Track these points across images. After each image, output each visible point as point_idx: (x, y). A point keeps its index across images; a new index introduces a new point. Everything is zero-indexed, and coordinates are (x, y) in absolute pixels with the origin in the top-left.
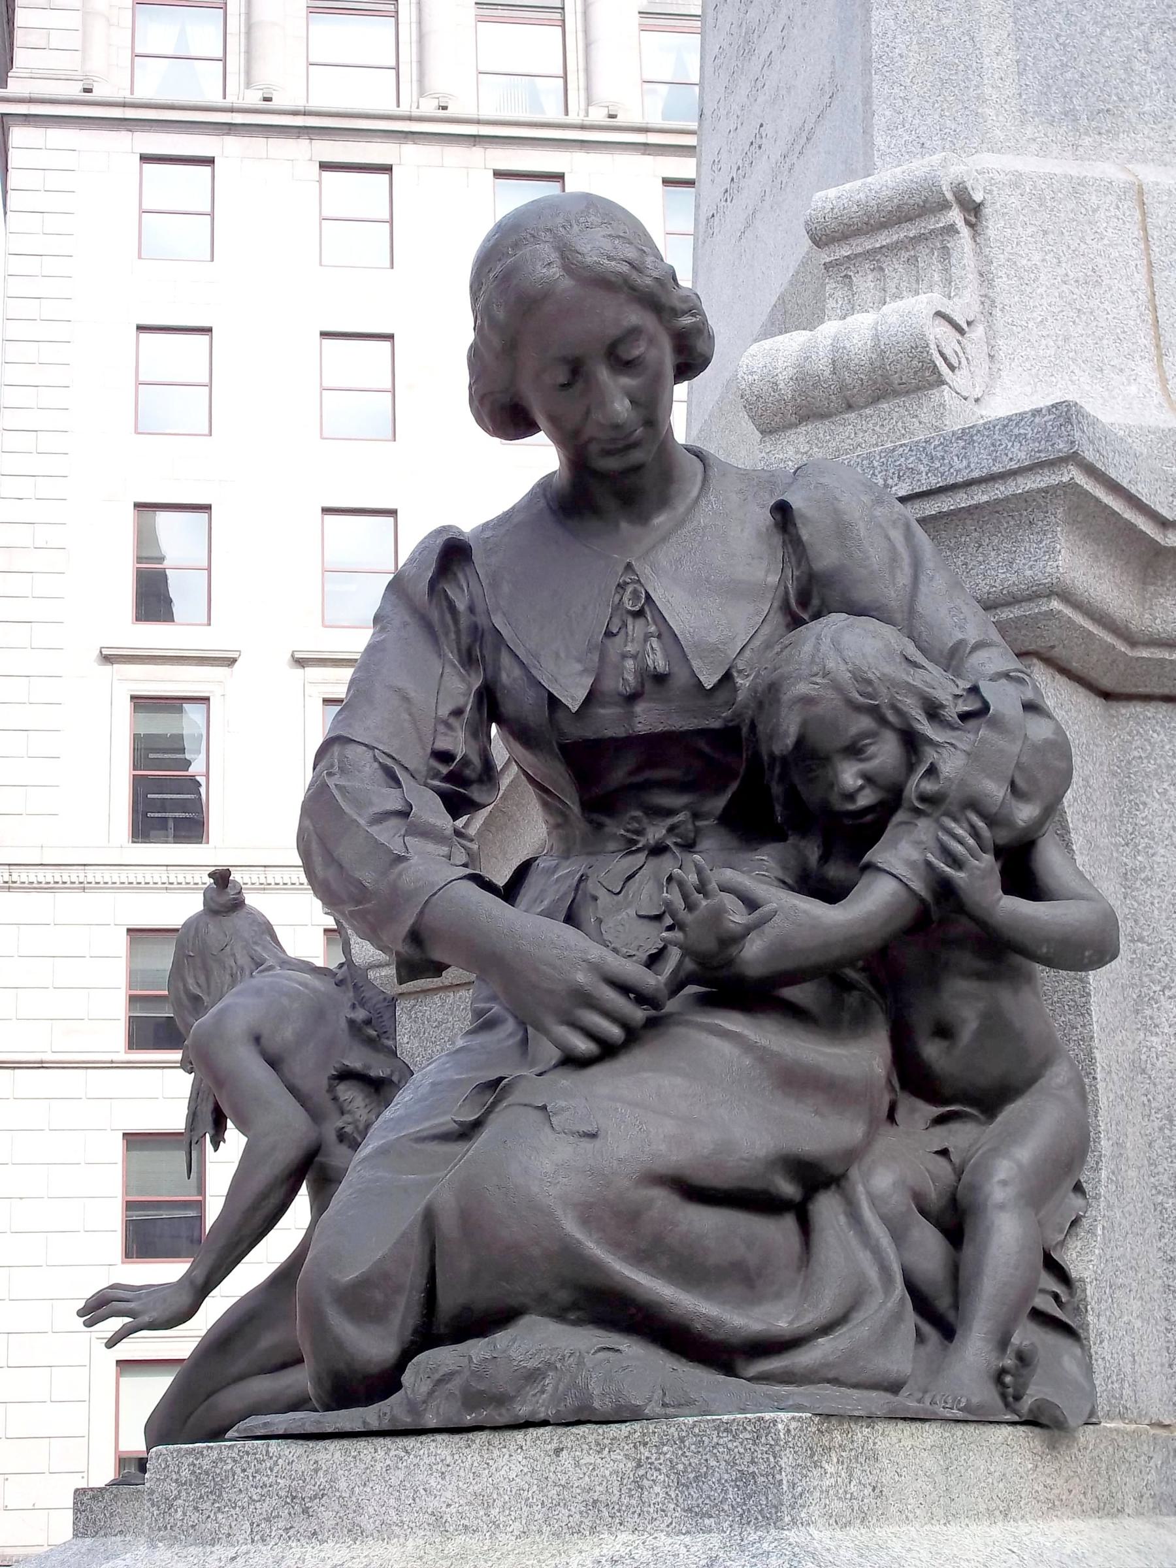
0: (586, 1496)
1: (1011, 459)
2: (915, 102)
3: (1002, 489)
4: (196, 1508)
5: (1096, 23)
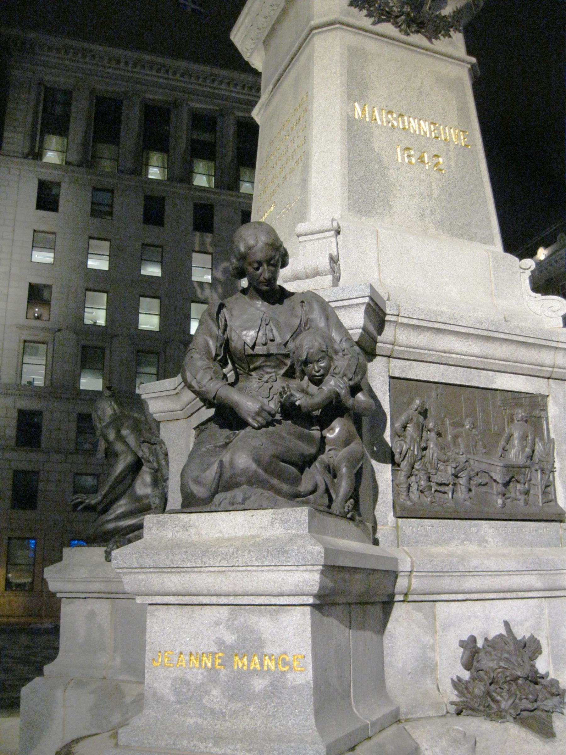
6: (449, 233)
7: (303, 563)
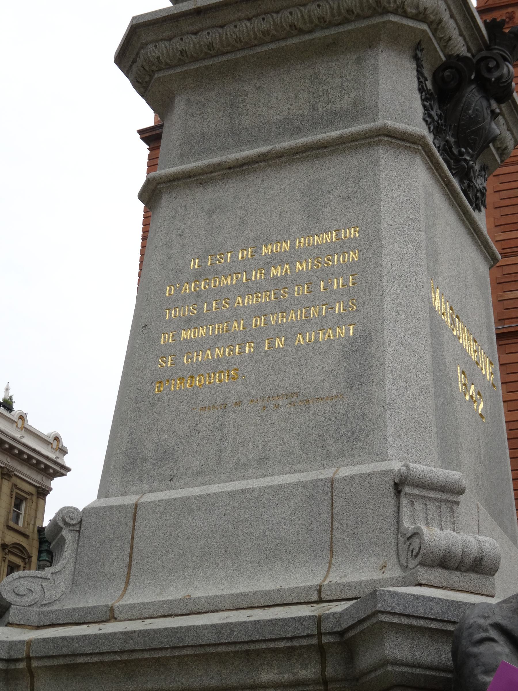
2: (405, 430)
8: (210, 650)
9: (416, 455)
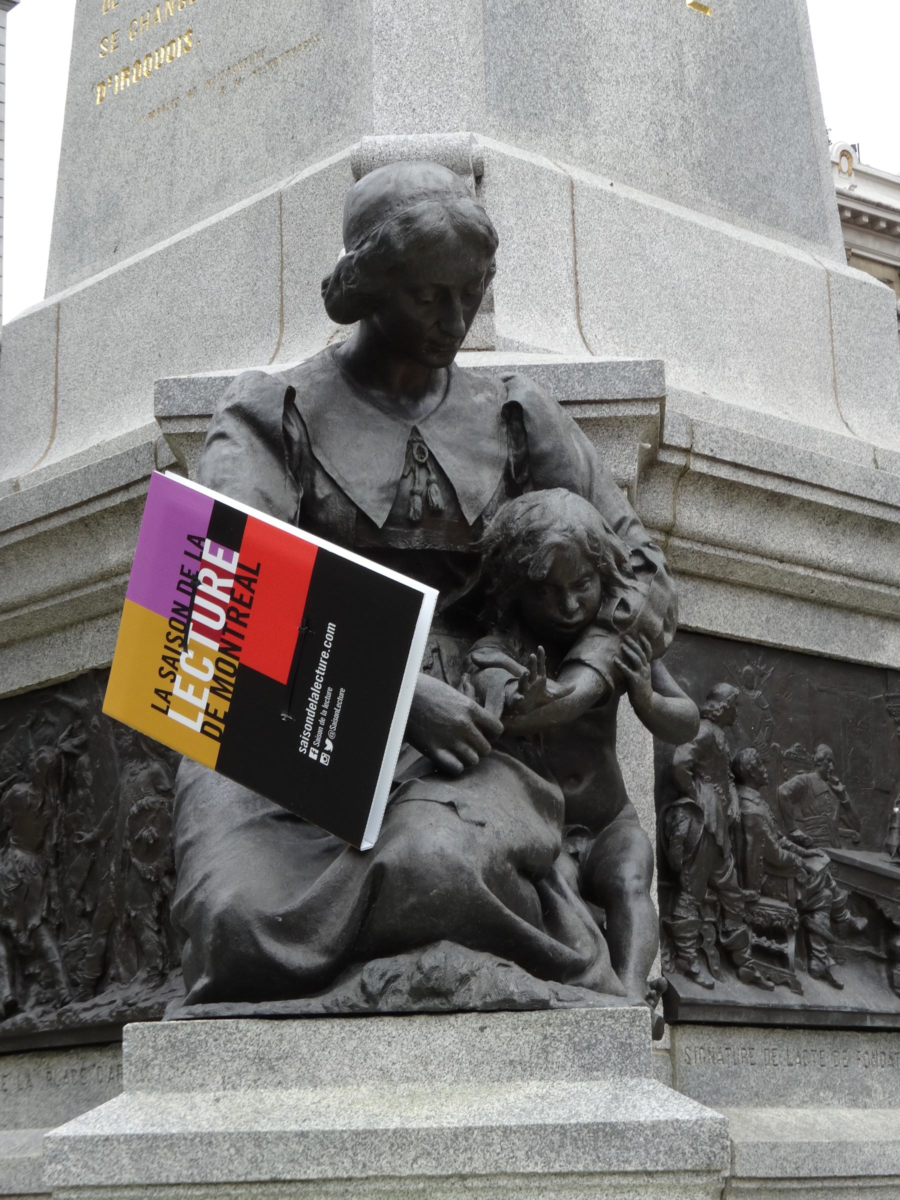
0: (504, 1057)
1: (618, 392)
2: (409, 75)
3: (608, 411)
4: (172, 1067)
5: (530, 46)
6: (723, 200)
7: (671, 1164)
8: (42, 527)
9: (431, 117)
